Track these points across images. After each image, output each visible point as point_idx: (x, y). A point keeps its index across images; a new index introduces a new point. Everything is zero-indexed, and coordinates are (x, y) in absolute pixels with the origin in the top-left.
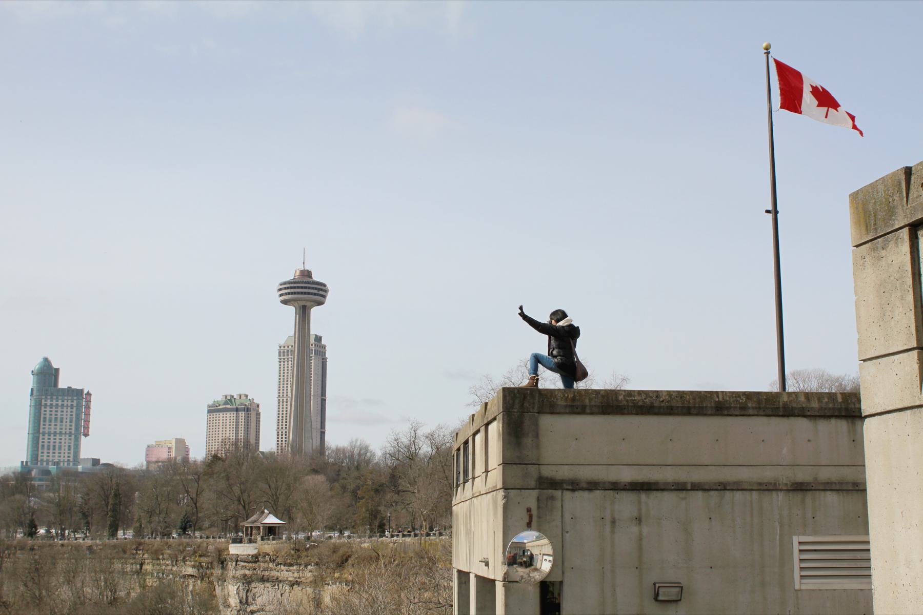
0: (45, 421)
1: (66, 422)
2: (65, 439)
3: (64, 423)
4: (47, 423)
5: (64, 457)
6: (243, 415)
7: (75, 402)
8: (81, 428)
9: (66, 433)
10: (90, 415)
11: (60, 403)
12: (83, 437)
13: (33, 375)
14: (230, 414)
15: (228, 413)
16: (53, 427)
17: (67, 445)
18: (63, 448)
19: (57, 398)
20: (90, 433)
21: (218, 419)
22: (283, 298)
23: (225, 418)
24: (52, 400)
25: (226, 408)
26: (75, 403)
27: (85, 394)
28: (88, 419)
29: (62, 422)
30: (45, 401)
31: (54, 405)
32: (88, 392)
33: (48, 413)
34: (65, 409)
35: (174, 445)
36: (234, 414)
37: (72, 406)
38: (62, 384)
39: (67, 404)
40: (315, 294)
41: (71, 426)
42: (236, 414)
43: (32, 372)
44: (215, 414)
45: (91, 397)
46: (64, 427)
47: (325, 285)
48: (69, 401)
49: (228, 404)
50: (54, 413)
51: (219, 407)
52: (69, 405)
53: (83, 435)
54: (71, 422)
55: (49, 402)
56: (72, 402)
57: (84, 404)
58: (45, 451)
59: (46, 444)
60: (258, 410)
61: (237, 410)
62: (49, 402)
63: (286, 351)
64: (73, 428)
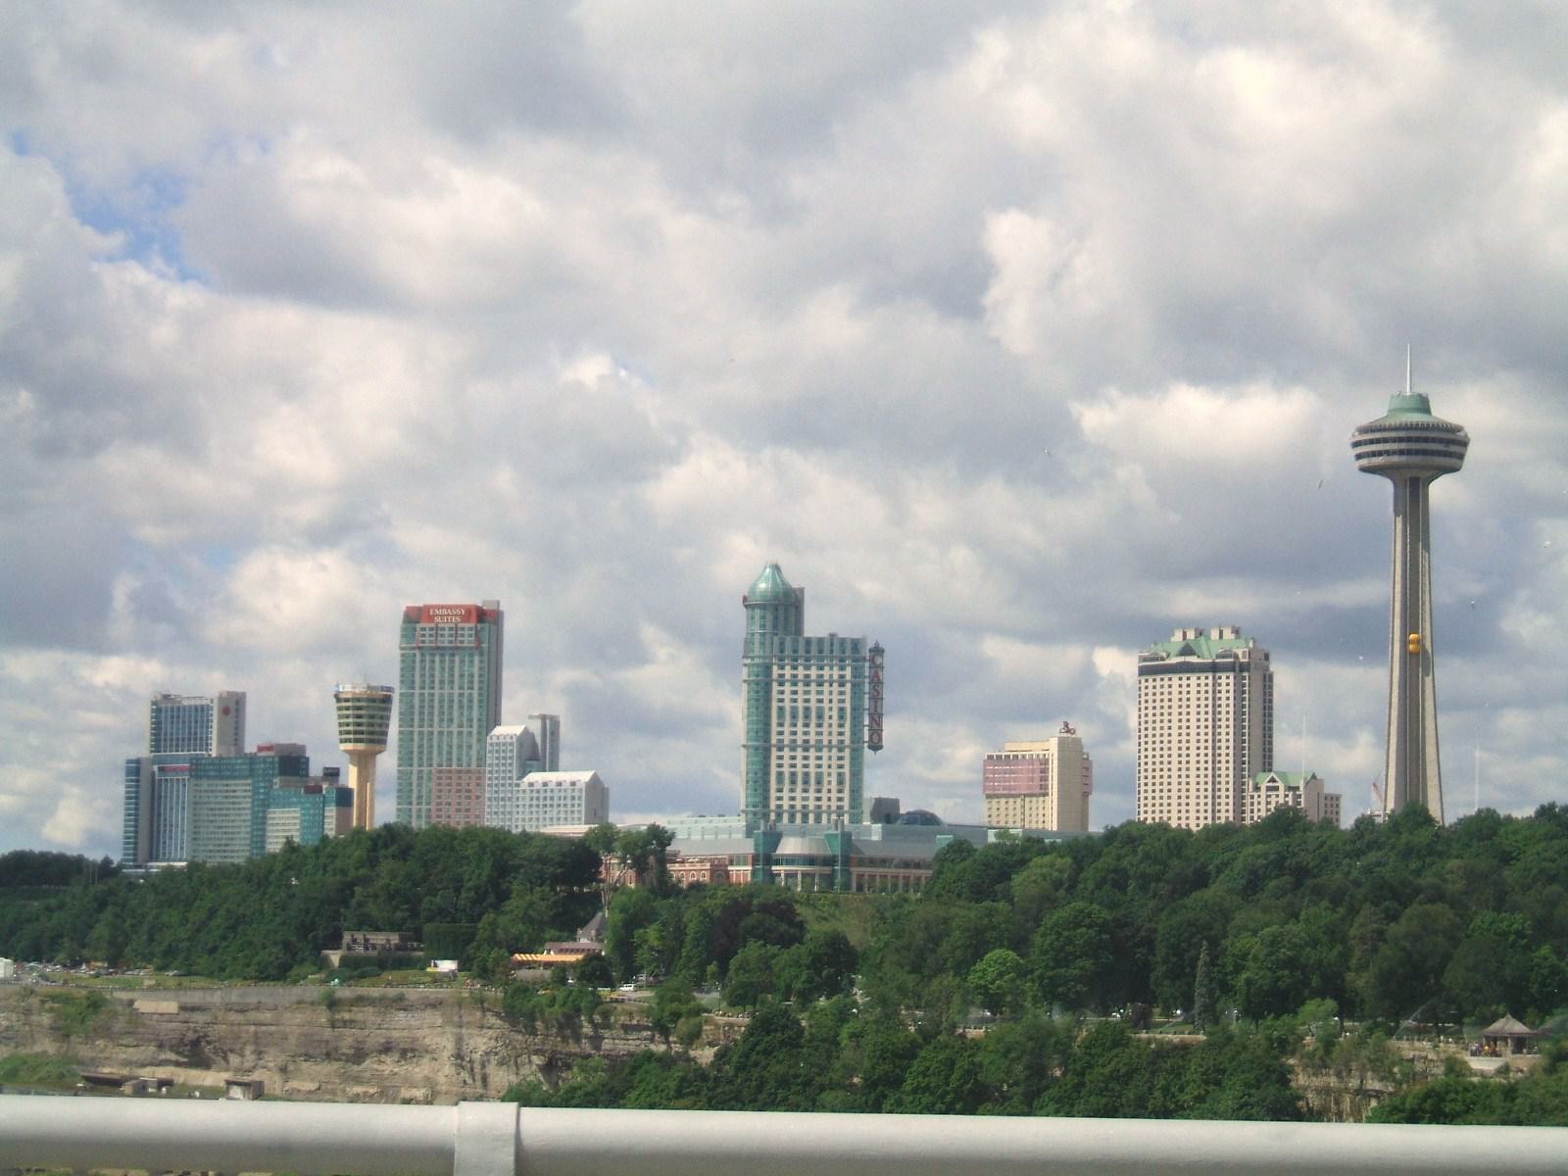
1: (830, 717)
3: (826, 721)
5: (829, 799)
6: (1231, 680)
9: (830, 747)
11: (814, 672)
12: (868, 753)
13: (746, 606)
15: (1194, 677)
17: (834, 771)
20: (884, 743)
21: (1166, 690)
22: (1364, 462)
23: (1184, 689)
25: (1184, 663)
26: (848, 672)
27: (870, 651)
28: (879, 710)
32: (877, 644)
33: (787, 696)
35: (1056, 756)
36: (1207, 678)
40: (1438, 453)
42: (1214, 678)
43: (745, 599)
44: (1158, 678)
47: (1459, 429)
49: (1192, 653)
50: (800, 697)
51: (1167, 662)
52: (835, 677)
53: (869, 747)
55: (788, 672)
56: (842, 668)
57: (867, 674)
59: (786, 770)
60: (1267, 668)
61: (1214, 668)
62: (788, 672)
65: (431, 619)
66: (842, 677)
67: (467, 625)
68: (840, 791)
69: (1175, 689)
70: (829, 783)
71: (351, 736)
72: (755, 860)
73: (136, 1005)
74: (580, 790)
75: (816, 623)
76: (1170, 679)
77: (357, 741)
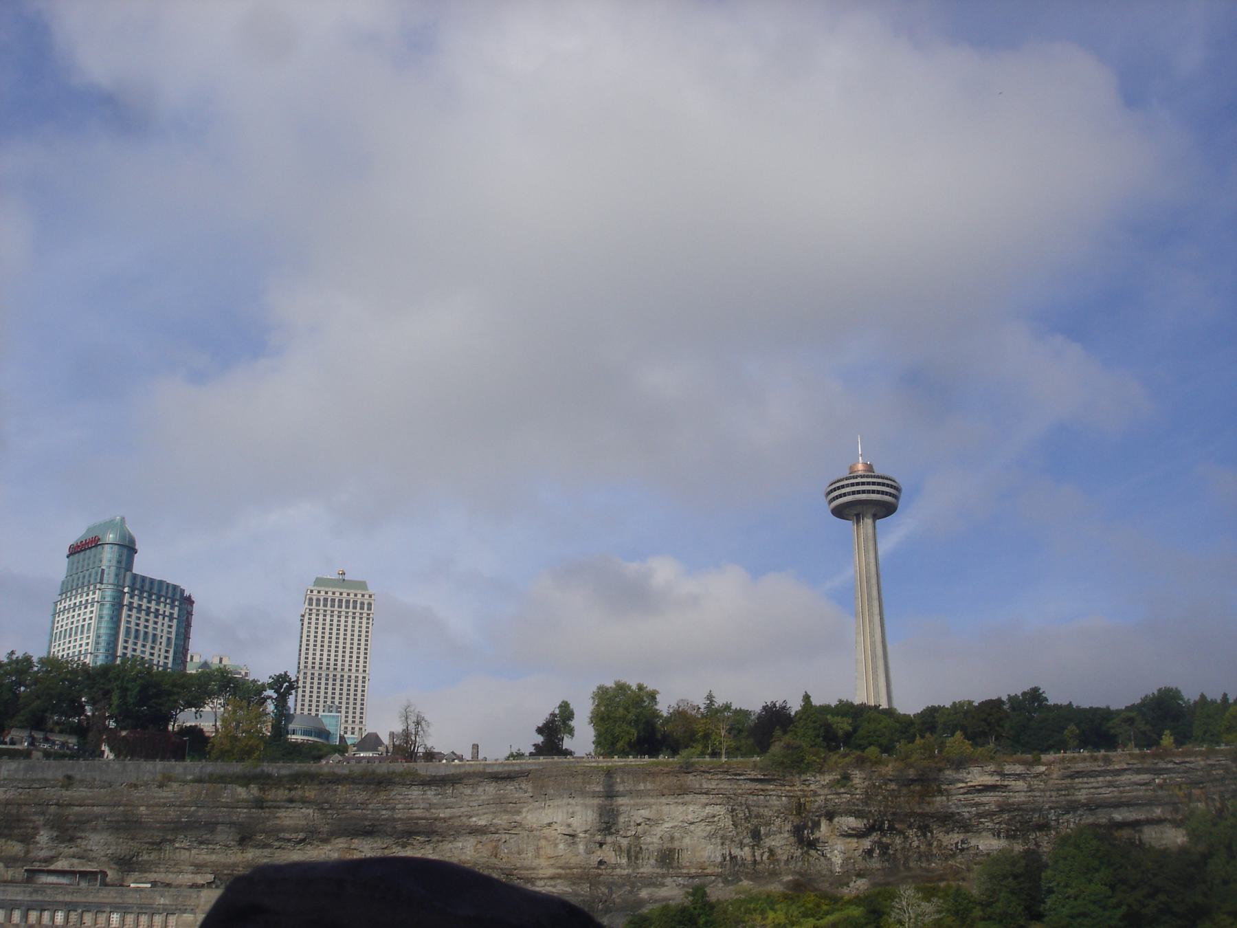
1: (161, 643)
7: (176, 609)
11: (153, 606)
19: (150, 595)
24: (141, 599)
29: (154, 642)
30: (132, 597)
37: (171, 617)
41: (167, 651)
45: (192, 606)
46: (156, 652)
52: (167, 614)
54: (168, 644)
55: (136, 601)
63: (322, 599)
64: (171, 655)
66: (171, 614)
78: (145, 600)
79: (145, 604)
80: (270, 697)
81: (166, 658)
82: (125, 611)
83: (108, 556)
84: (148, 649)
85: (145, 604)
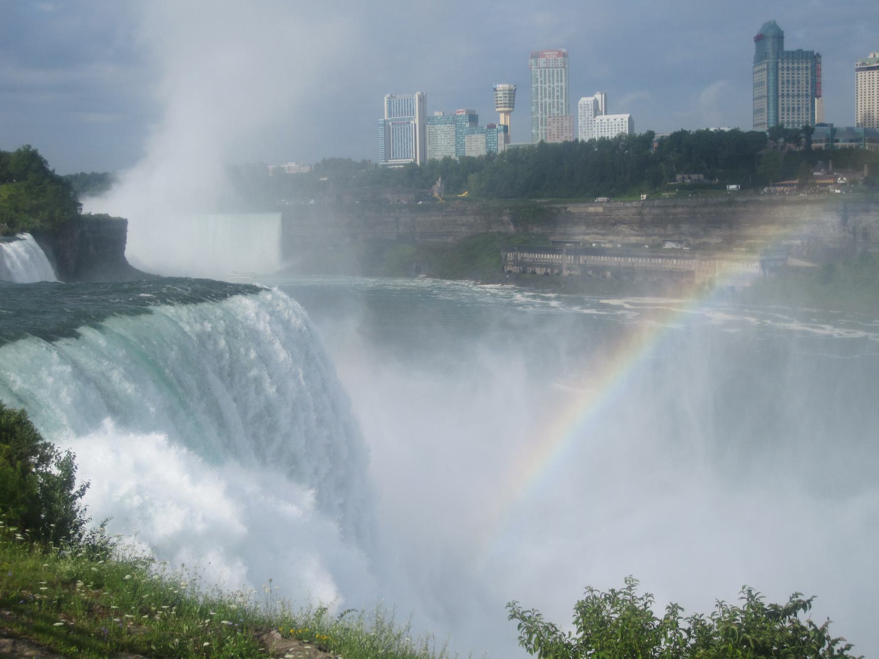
0: (783, 83)
2: (803, 101)
3: (801, 86)
4: (785, 85)
7: (809, 64)
8: (816, 91)
10: (821, 77)
11: (796, 65)
14: (865, 73)
16: (791, 89)
17: (805, 106)
18: (801, 109)
24: (788, 63)
26: (809, 65)
30: (783, 64)
31: (790, 67)
34: (801, 72)
38: (788, 46)
39: (802, 67)
46: (801, 89)
48: (804, 64)
54: (807, 83)
58: (786, 113)
64: (809, 89)
65: (544, 56)
67: (559, 58)
68: (807, 114)
69: (867, 77)
70: (803, 111)
71: (502, 105)
72: (827, 140)
73: (568, 209)
74: (626, 122)
75: (788, 46)
76: (873, 73)
77: (505, 107)
78: (791, 63)
79: (790, 65)
80: (803, 137)
81: (807, 91)
82: (780, 72)
83: (769, 45)
84: (796, 89)
85: (790, 65)
